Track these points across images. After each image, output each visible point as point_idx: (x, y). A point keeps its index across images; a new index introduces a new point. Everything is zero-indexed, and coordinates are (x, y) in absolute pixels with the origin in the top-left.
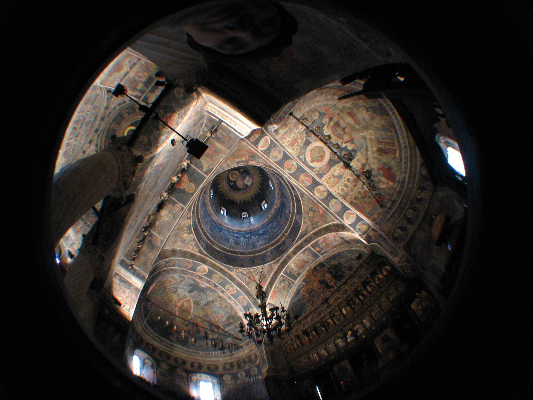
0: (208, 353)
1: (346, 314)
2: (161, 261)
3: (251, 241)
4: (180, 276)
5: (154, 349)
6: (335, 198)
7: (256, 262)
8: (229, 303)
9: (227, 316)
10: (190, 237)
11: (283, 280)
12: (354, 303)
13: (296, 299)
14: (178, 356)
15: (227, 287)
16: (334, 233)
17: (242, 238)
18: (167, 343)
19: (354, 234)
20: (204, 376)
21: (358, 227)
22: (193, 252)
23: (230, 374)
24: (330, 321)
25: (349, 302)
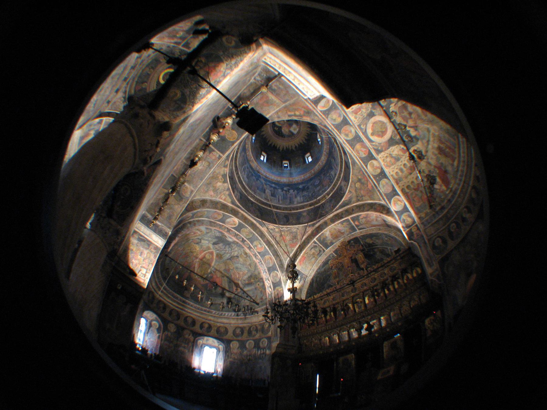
0: (221, 313)
1: (368, 304)
2: (187, 214)
3: (289, 196)
4: (207, 228)
5: (165, 307)
6: (387, 178)
7: (291, 221)
8: (254, 261)
9: (249, 274)
10: (223, 186)
11: (315, 247)
13: (323, 270)
14: (189, 314)
15: (255, 243)
16: (378, 214)
17: (280, 190)
18: (181, 300)
19: (397, 223)
20: (211, 340)
21: (403, 217)
22: (225, 202)
23: (238, 341)
25: (373, 293)
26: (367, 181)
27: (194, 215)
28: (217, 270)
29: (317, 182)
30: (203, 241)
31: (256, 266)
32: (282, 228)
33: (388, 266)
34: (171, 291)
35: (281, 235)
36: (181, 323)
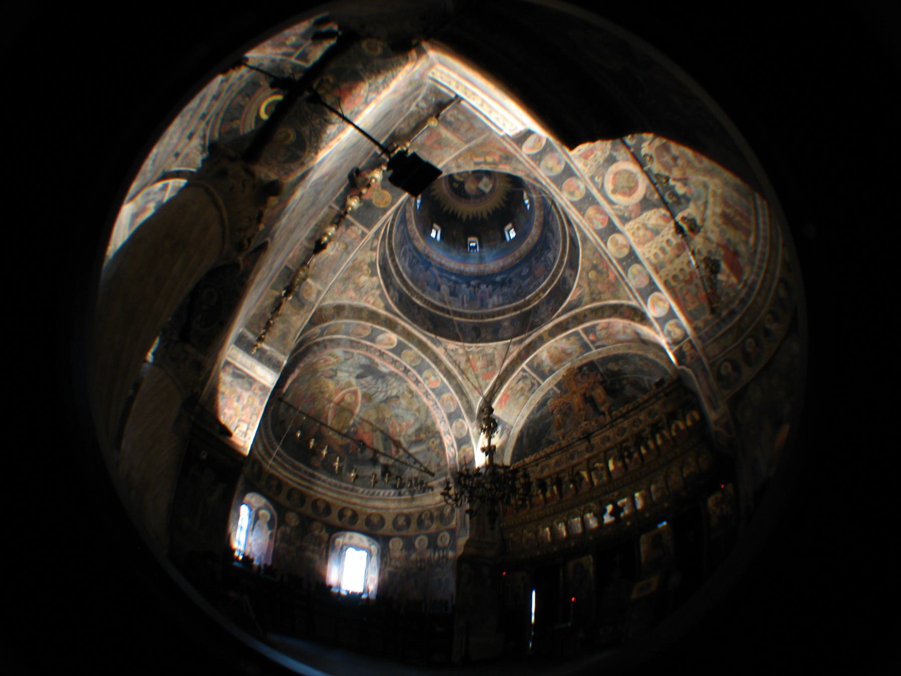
0: (372, 491)
2: (313, 329)
3: (479, 294)
4: (346, 352)
5: (280, 484)
7: (483, 335)
8: (424, 405)
9: (417, 426)
11: (524, 378)
12: (630, 456)
13: (538, 415)
14: (319, 496)
15: (426, 374)
16: (626, 322)
17: (464, 286)
18: (305, 472)
20: (357, 538)
23: (402, 537)
24: (585, 474)
25: (622, 454)
26: (608, 268)
27: (323, 330)
28: (363, 420)
29: (525, 271)
30: (339, 374)
31: (428, 412)
32: (470, 347)
33: (644, 408)
34: (289, 458)
35: (468, 360)
36: (308, 510)
